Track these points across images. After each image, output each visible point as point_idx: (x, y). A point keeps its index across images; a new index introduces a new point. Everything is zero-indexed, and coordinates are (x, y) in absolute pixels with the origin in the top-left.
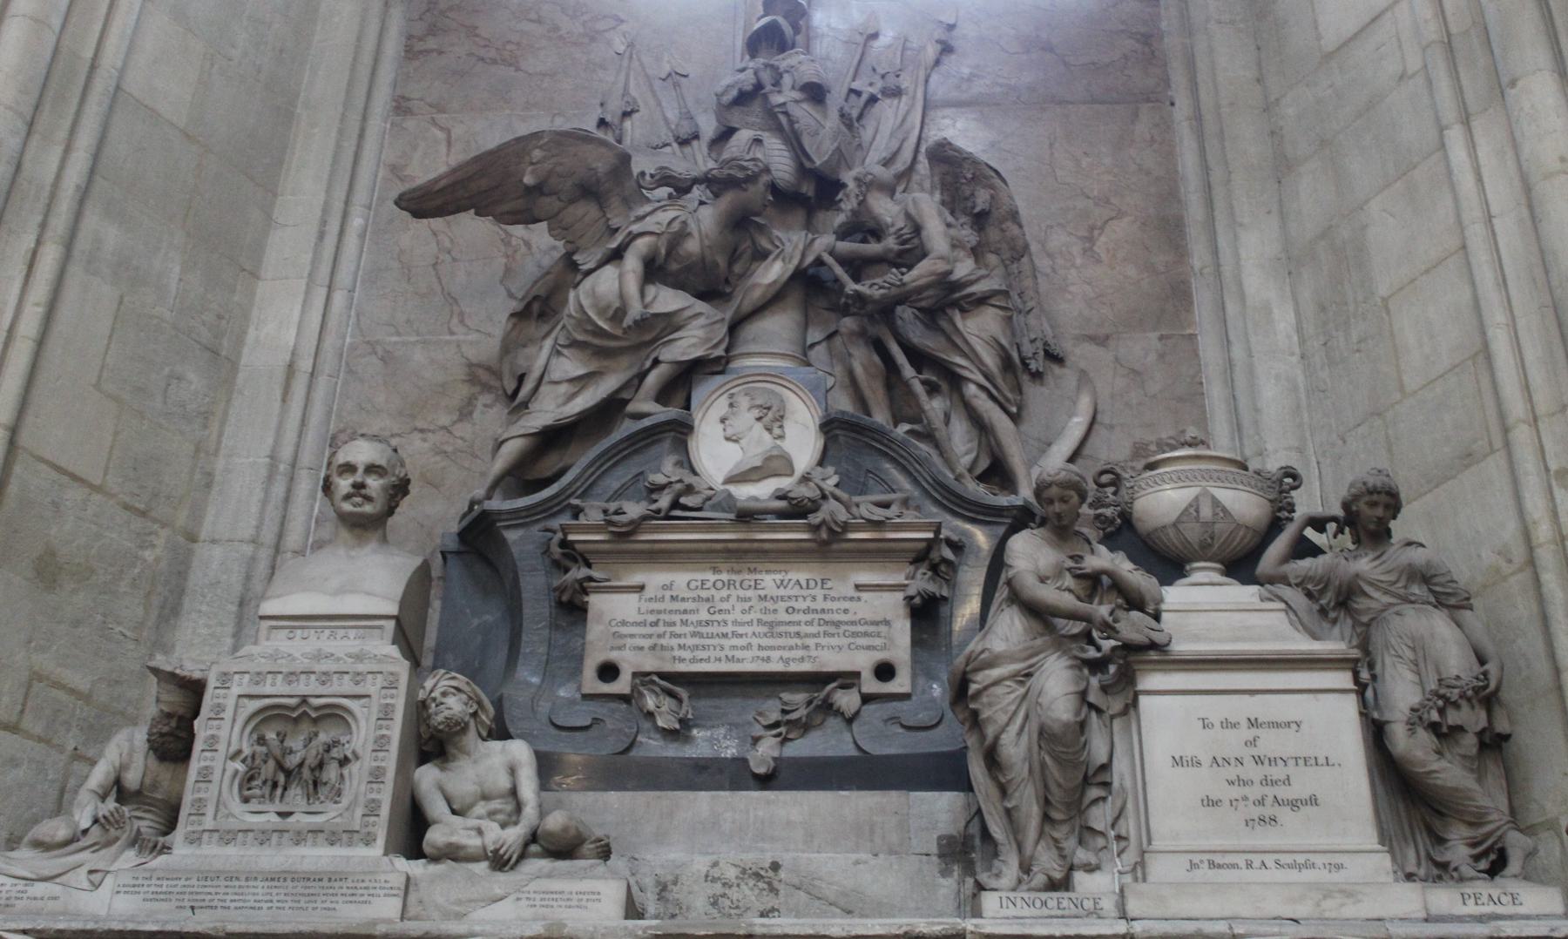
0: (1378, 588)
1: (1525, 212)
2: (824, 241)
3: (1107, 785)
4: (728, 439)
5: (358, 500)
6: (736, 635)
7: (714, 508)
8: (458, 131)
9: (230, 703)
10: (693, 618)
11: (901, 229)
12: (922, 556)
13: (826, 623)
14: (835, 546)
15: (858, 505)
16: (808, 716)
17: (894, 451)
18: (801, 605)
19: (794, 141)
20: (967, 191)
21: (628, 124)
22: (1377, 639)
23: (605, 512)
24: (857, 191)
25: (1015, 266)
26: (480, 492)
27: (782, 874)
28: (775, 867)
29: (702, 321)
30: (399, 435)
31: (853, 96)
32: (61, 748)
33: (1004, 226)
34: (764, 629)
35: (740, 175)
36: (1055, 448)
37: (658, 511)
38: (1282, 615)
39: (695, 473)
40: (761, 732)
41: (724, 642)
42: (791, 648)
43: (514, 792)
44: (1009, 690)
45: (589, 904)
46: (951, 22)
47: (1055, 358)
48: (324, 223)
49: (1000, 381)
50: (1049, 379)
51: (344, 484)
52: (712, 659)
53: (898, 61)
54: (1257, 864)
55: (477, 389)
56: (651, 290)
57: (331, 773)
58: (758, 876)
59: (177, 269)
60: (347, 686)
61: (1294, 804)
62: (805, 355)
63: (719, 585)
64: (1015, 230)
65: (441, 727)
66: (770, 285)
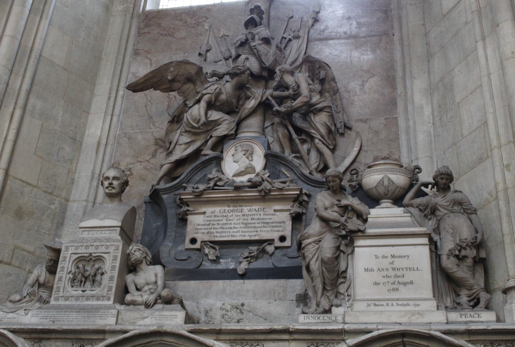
0: (443, 208)
1: (501, 72)
2: (269, 92)
3: (345, 278)
4: (234, 162)
5: (110, 188)
6: (234, 228)
7: (228, 186)
8: (154, 60)
9: (68, 256)
10: (221, 222)
11: (294, 87)
12: (296, 199)
13: (264, 223)
14: (267, 197)
15: (274, 183)
16: (257, 254)
17: (289, 164)
18: (256, 217)
19: (259, 58)
20: (317, 72)
21: (208, 54)
22: (442, 226)
23: (193, 188)
24: (279, 74)
25: (334, 96)
26: (155, 182)
27: (245, 307)
28: (243, 305)
29: (227, 122)
30: (133, 164)
31: (284, 39)
32: (25, 270)
33: (331, 83)
34: (243, 226)
35: (238, 72)
36: (346, 159)
37: (210, 187)
38: (409, 218)
42: (252, 232)
43: (156, 282)
44: (313, 246)
45: (174, 319)
46: (318, 10)
48: (110, 93)
49: (326, 138)
50: (346, 135)
51: (106, 183)
52: (227, 236)
53: (299, 26)
54: (390, 304)
55: (158, 147)
56: (210, 113)
57: (98, 277)
58: (237, 308)
59: (61, 113)
60: (103, 249)
61: (405, 284)
62: (264, 131)
63: (230, 211)
64: (334, 84)
65: (133, 262)
66: (251, 108)
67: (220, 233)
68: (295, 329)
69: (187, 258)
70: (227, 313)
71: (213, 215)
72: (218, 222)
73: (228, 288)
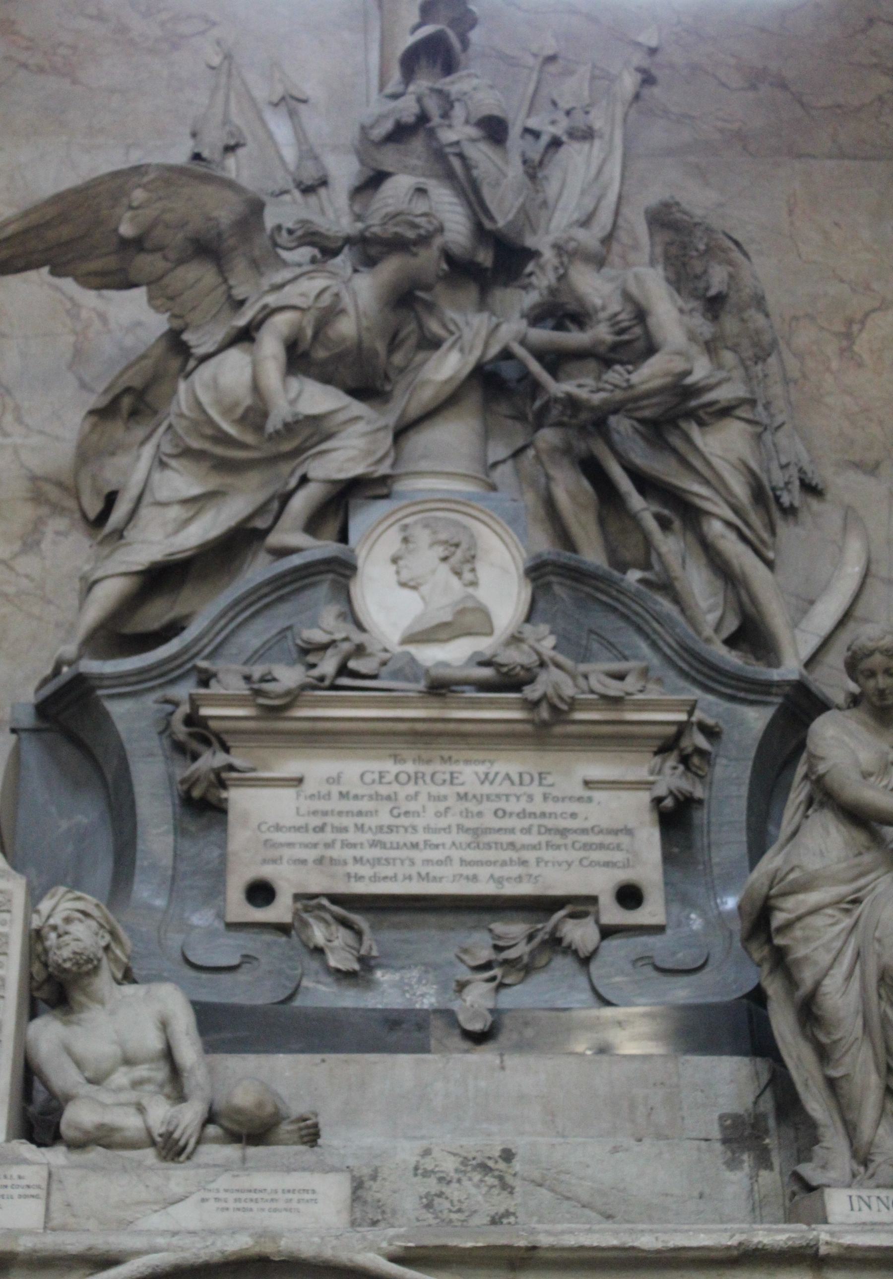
4: (403, 585)
6: (428, 844)
7: (396, 675)
11: (616, 315)
13: (548, 831)
14: (558, 730)
15: (586, 677)
16: (532, 954)
17: (623, 604)
20: (698, 266)
23: (248, 678)
24: (555, 261)
25: (759, 367)
26: (70, 649)
27: (517, 1165)
28: (508, 1155)
29: (361, 427)
33: (746, 315)
35: (411, 234)
37: (322, 679)
39: (360, 626)
40: (467, 975)
41: (413, 854)
42: (504, 864)
43: (169, 1055)
44: (830, 921)
45: (302, 1207)
46: (653, 43)
47: (811, 489)
50: (804, 516)
52: (400, 877)
53: (586, 93)
55: (44, 510)
56: (295, 383)
58: (484, 1168)
63: (403, 778)
64: (760, 320)
65: (68, 965)
67: (373, 866)
68: (840, 1246)
69: (235, 961)
70: (446, 1190)
71: (335, 790)
72: (360, 820)
73: (439, 1085)
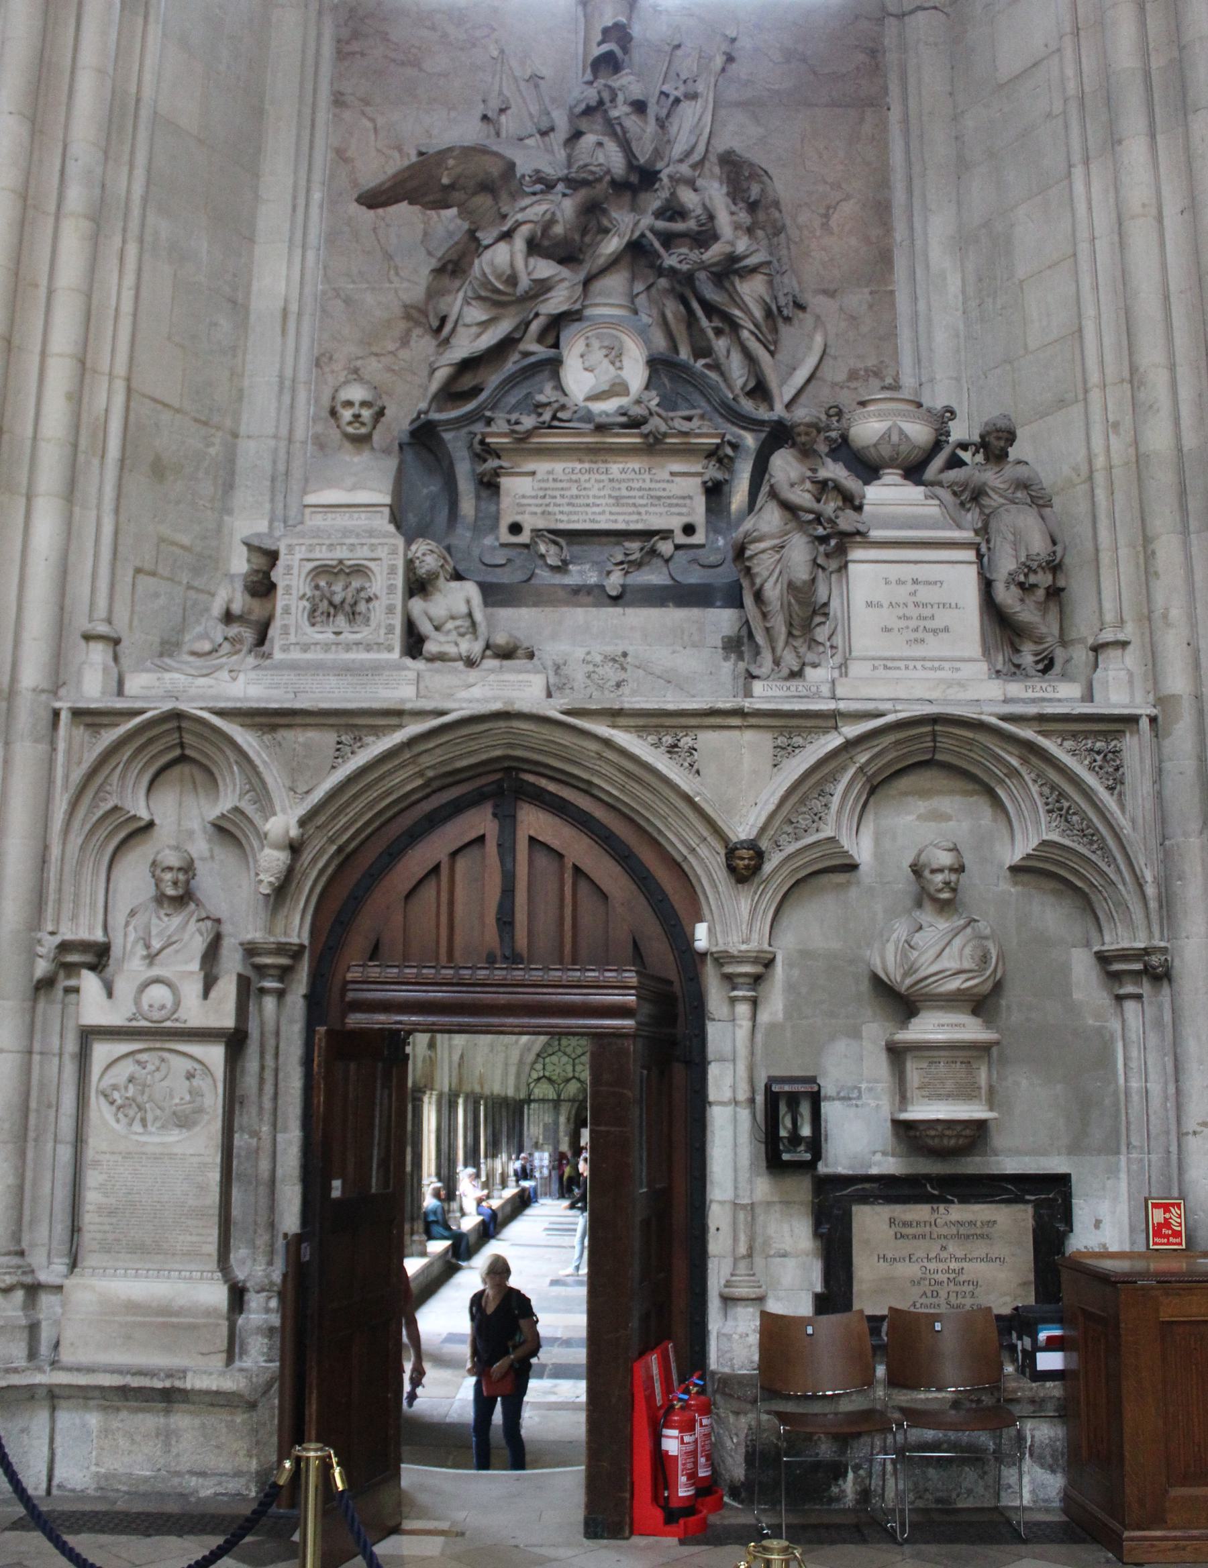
0: (996, 493)
1: (1116, 238)
2: (647, 221)
3: (826, 615)
4: (586, 369)
5: (357, 425)
7: (581, 420)
8: (380, 121)
9: (296, 564)
10: (567, 493)
12: (713, 454)
14: (658, 447)
16: (642, 557)
18: (636, 485)
19: (626, 146)
20: (745, 185)
21: (503, 118)
22: (993, 525)
23: (509, 421)
27: (629, 659)
28: (625, 655)
29: (566, 284)
30: (361, 358)
31: (663, 97)
32: (180, 583)
34: (612, 501)
35: (591, 178)
36: (798, 372)
37: (544, 423)
38: (937, 509)
40: (612, 568)
41: (588, 509)
42: (630, 514)
43: (470, 615)
46: (734, 35)
47: (800, 306)
48: (295, 198)
49: (764, 329)
50: (795, 322)
51: (347, 414)
54: (911, 667)
55: (411, 324)
56: (532, 261)
57: (362, 607)
58: (614, 660)
59: (205, 244)
60: (365, 552)
61: (935, 631)
62: (633, 302)
64: (777, 215)
66: (610, 255)
71: (551, 477)
